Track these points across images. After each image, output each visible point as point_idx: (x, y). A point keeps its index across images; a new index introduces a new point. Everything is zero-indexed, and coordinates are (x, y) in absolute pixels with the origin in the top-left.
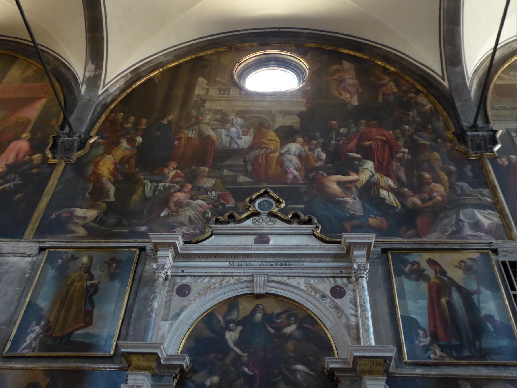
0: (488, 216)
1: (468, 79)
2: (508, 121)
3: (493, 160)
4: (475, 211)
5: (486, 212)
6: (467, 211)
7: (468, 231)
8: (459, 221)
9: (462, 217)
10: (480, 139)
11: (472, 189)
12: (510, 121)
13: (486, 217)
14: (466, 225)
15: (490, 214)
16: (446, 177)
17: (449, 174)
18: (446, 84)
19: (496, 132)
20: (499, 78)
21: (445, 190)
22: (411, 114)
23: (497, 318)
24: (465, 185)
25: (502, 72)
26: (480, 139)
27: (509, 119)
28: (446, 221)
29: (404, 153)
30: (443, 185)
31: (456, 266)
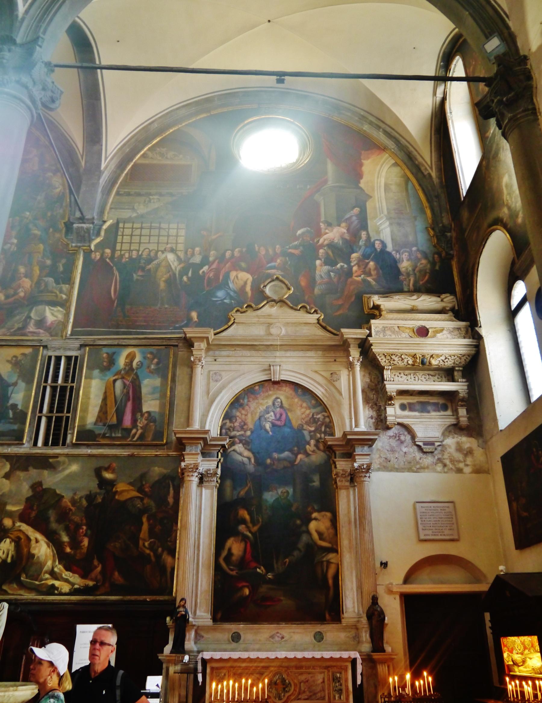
0: (56, 314)
1: (106, 158)
2: (124, 209)
3: (88, 253)
4: (47, 308)
5: (55, 309)
6: (40, 307)
7: (31, 328)
8: (29, 317)
9: (32, 315)
10: (84, 231)
11: (54, 285)
12: (126, 209)
13: (53, 314)
14: (32, 323)
15: (59, 311)
16: (38, 272)
17: (42, 267)
18: (83, 163)
19: (105, 222)
20: (144, 156)
21: (31, 286)
22: (39, 198)
23: (20, 407)
24: (51, 280)
25: (149, 149)
26: (84, 231)
27: (127, 207)
28: (18, 317)
29: (12, 244)
30: (32, 281)
31: (8, 361)
